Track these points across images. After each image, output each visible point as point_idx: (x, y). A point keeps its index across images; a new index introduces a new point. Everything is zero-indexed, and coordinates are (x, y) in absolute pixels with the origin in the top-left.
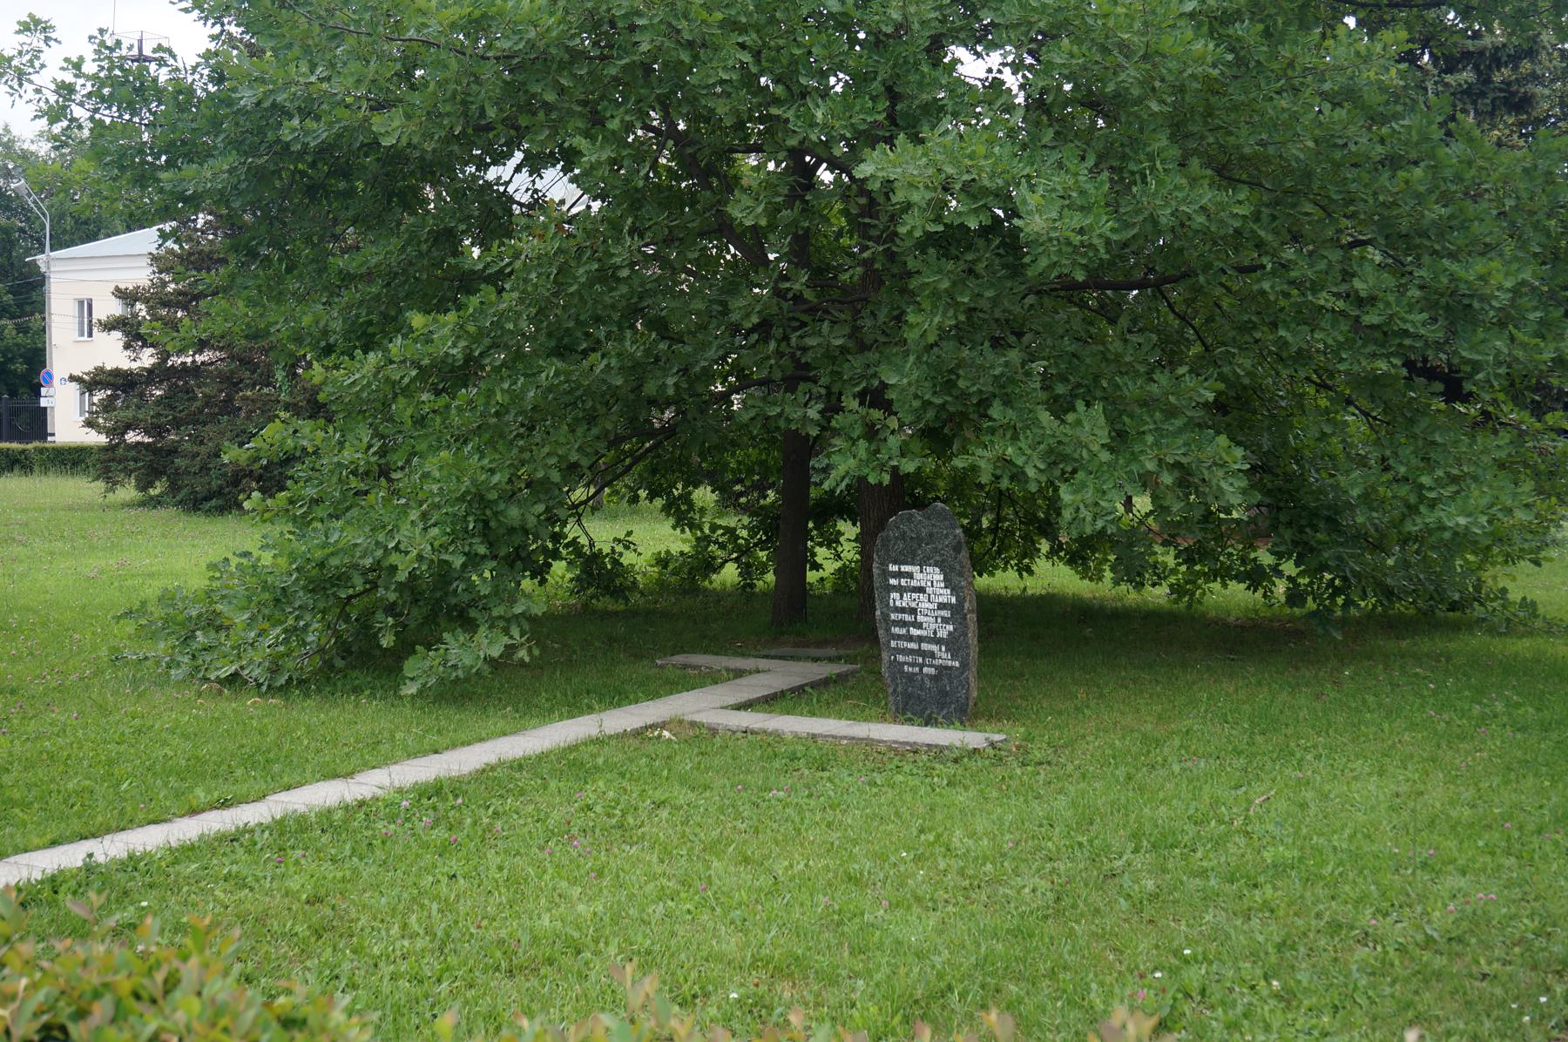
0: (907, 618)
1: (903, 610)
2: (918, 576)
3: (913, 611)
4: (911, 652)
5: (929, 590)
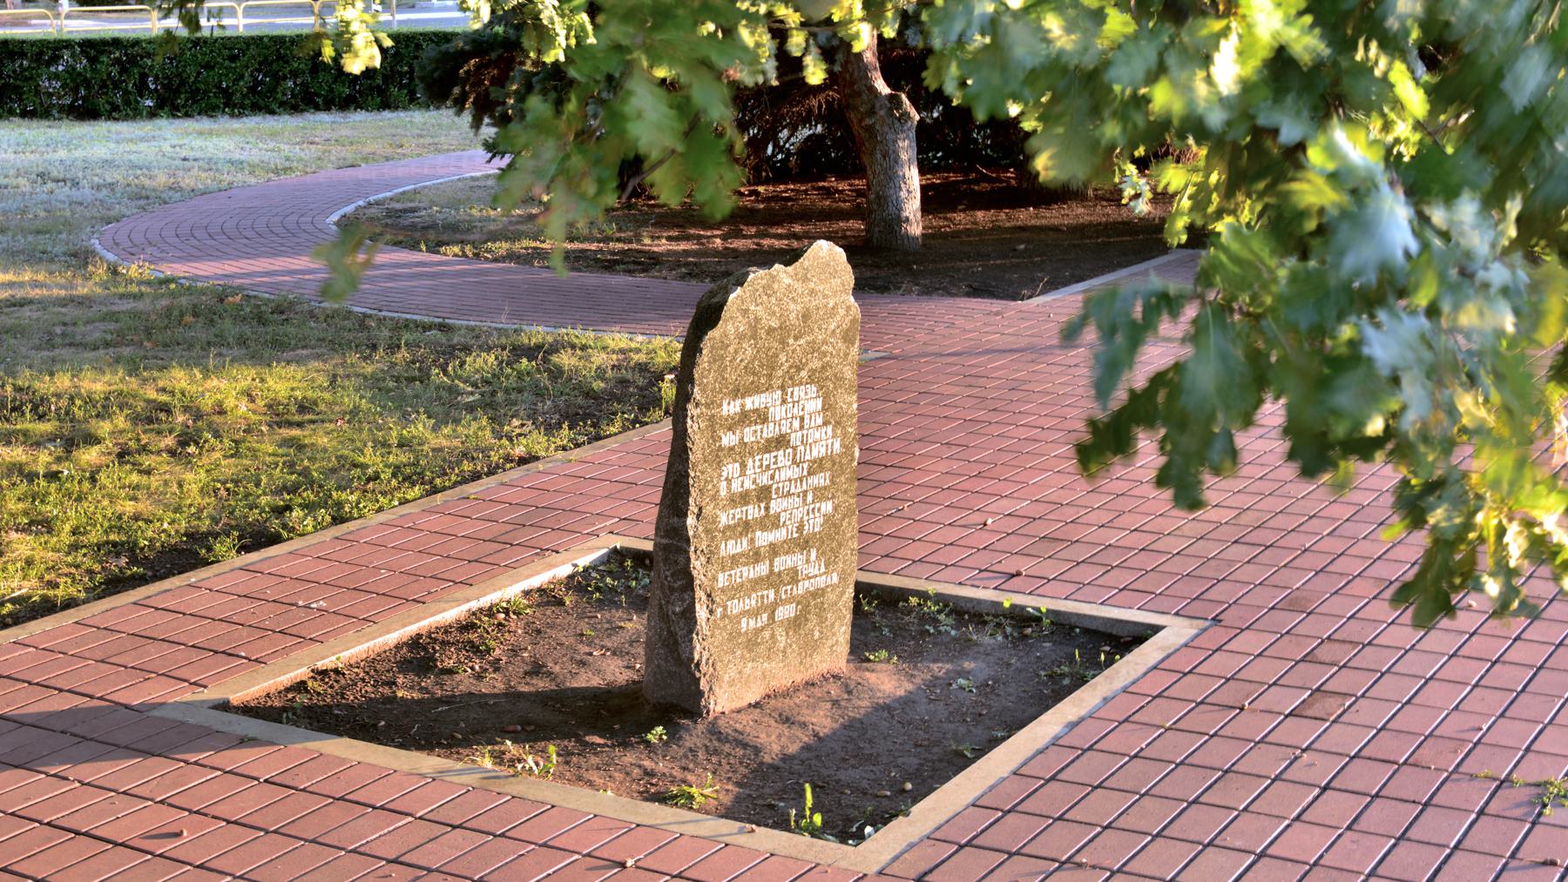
0: (753, 512)
2: (777, 412)
5: (795, 439)
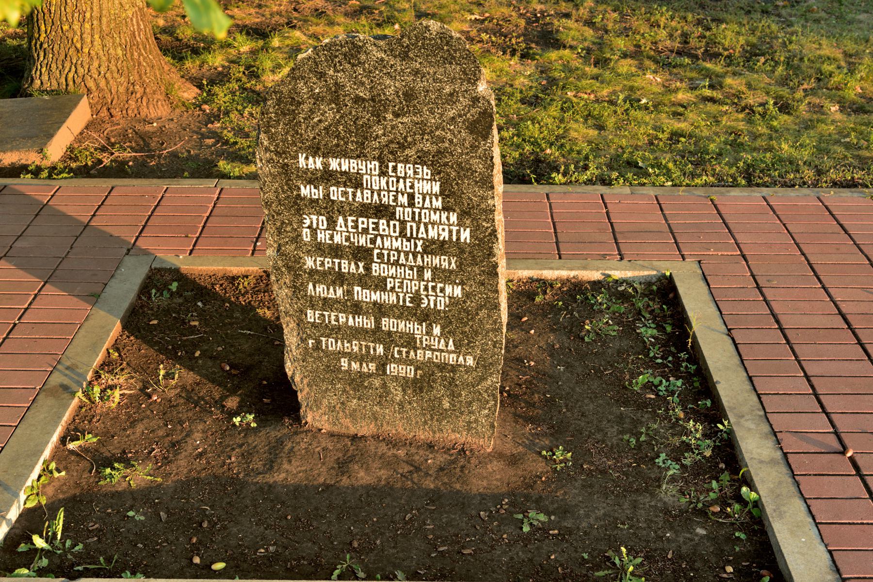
1: (336, 251)
3: (362, 254)
4: (357, 333)
